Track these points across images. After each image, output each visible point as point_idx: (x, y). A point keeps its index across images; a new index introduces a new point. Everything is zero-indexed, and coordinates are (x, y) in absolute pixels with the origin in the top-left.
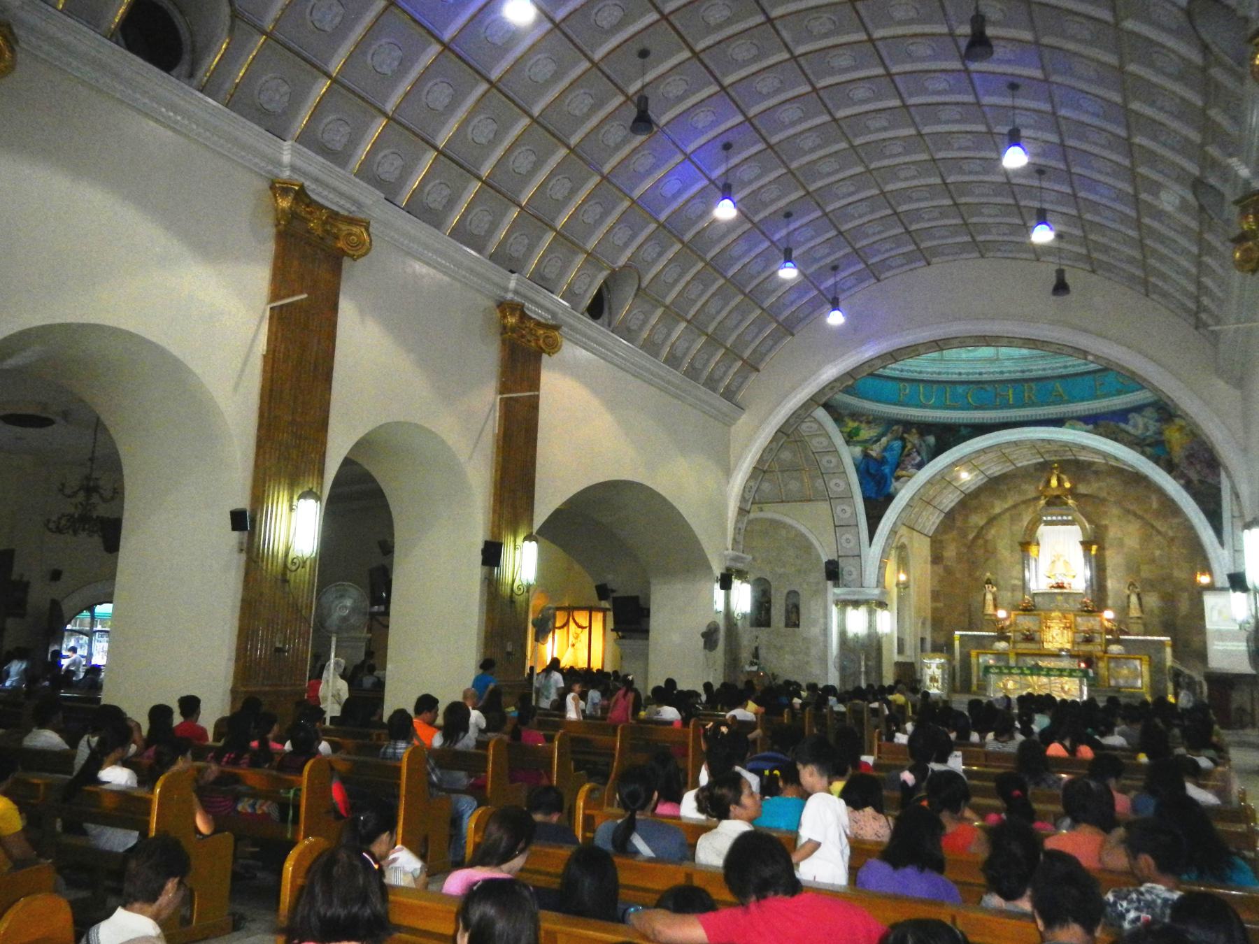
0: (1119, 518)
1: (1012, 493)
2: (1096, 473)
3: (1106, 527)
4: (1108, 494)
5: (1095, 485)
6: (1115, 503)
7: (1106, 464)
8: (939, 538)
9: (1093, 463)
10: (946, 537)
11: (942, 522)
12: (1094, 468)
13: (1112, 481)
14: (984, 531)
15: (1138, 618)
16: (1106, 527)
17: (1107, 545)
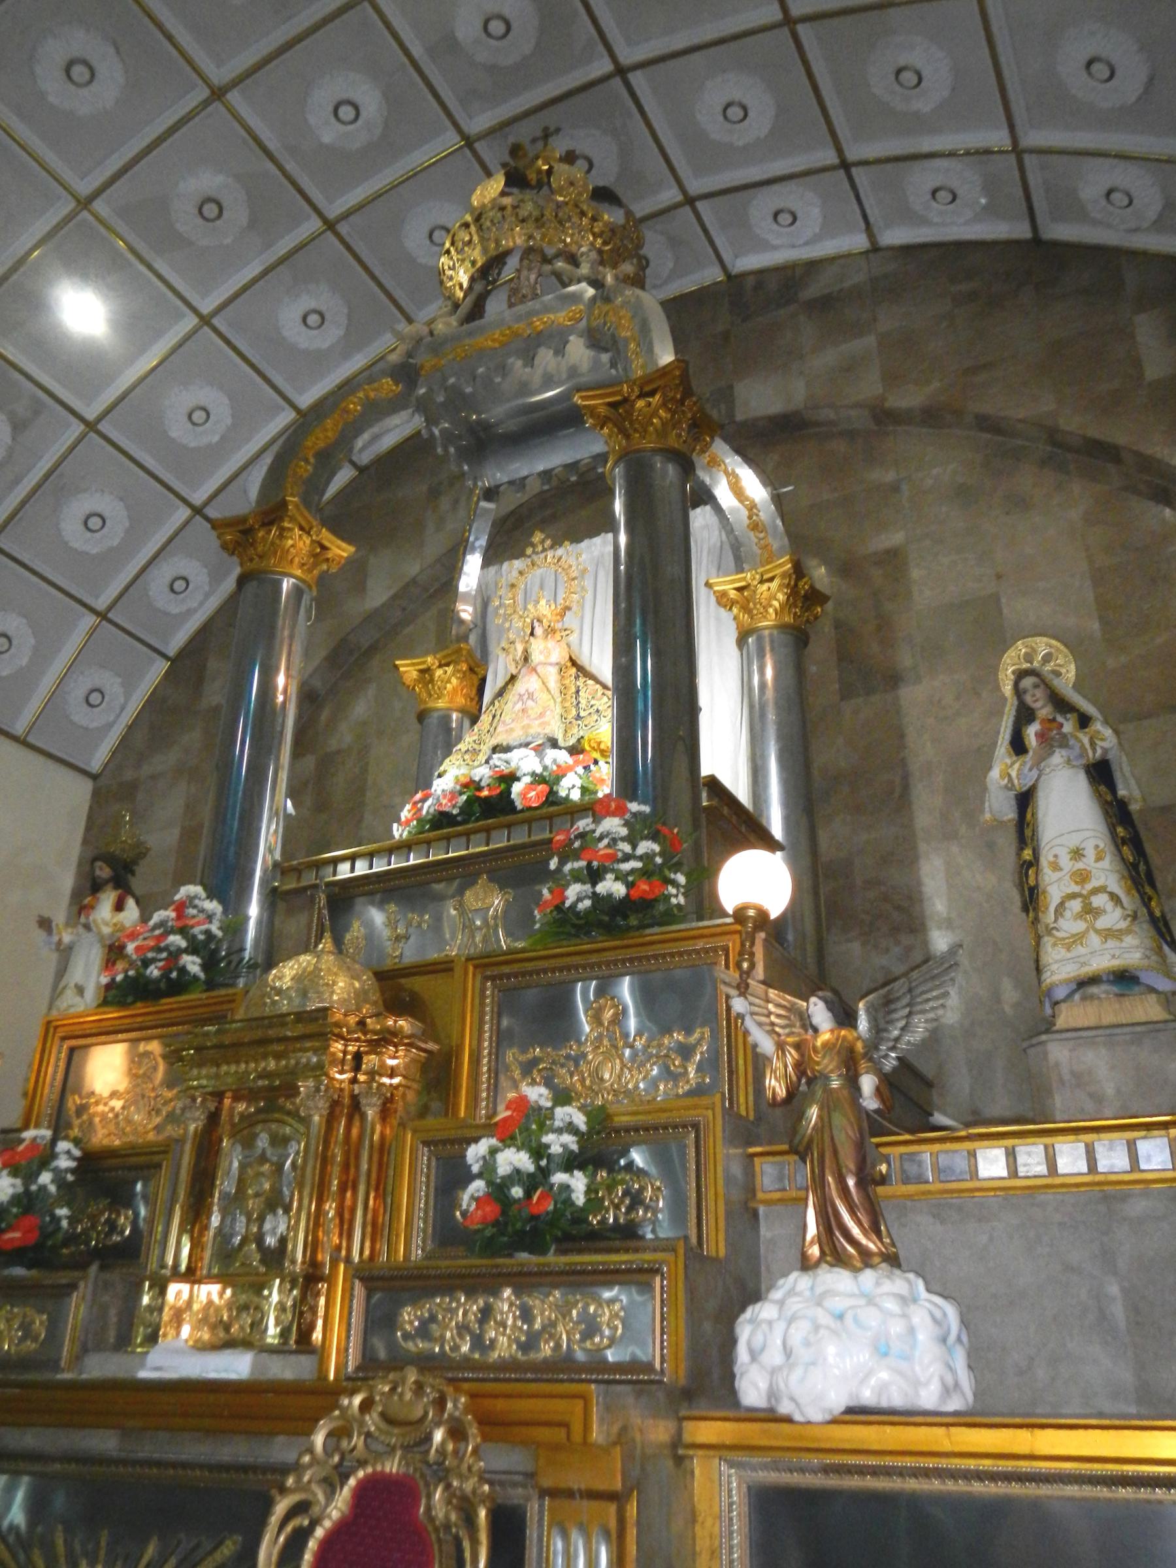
0: (964, 494)
1: (445, 503)
2: (825, 304)
3: (893, 559)
4: (892, 379)
5: (827, 358)
6: (931, 417)
7: (875, 248)
8: (129, 775)
9: (813, 266)
10: (164, 761)
11: (155, 702)
12: (813, 291)
13: (889, 319)
14: (325, 715)
15: (1124, 979)
16: (893, 559)
17: (905, 659)
